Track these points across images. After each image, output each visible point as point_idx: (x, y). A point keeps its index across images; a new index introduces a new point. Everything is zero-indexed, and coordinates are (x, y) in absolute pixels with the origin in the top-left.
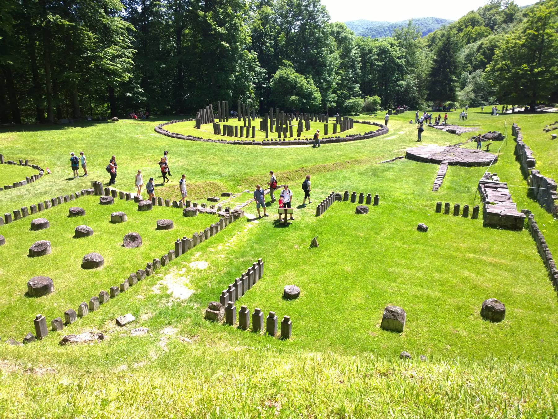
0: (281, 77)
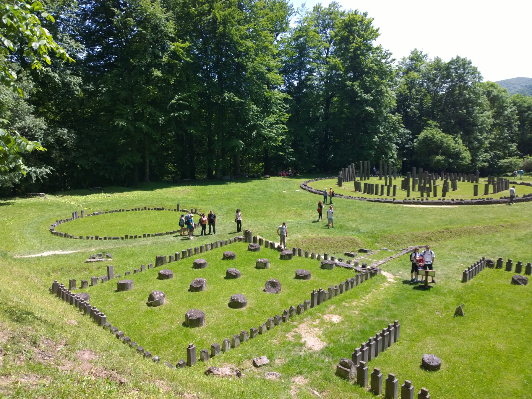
0: (426, 138)
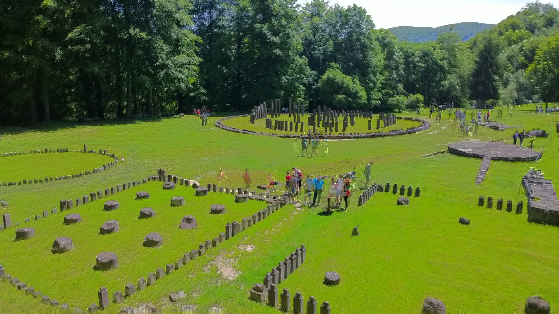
0: (329, 79)
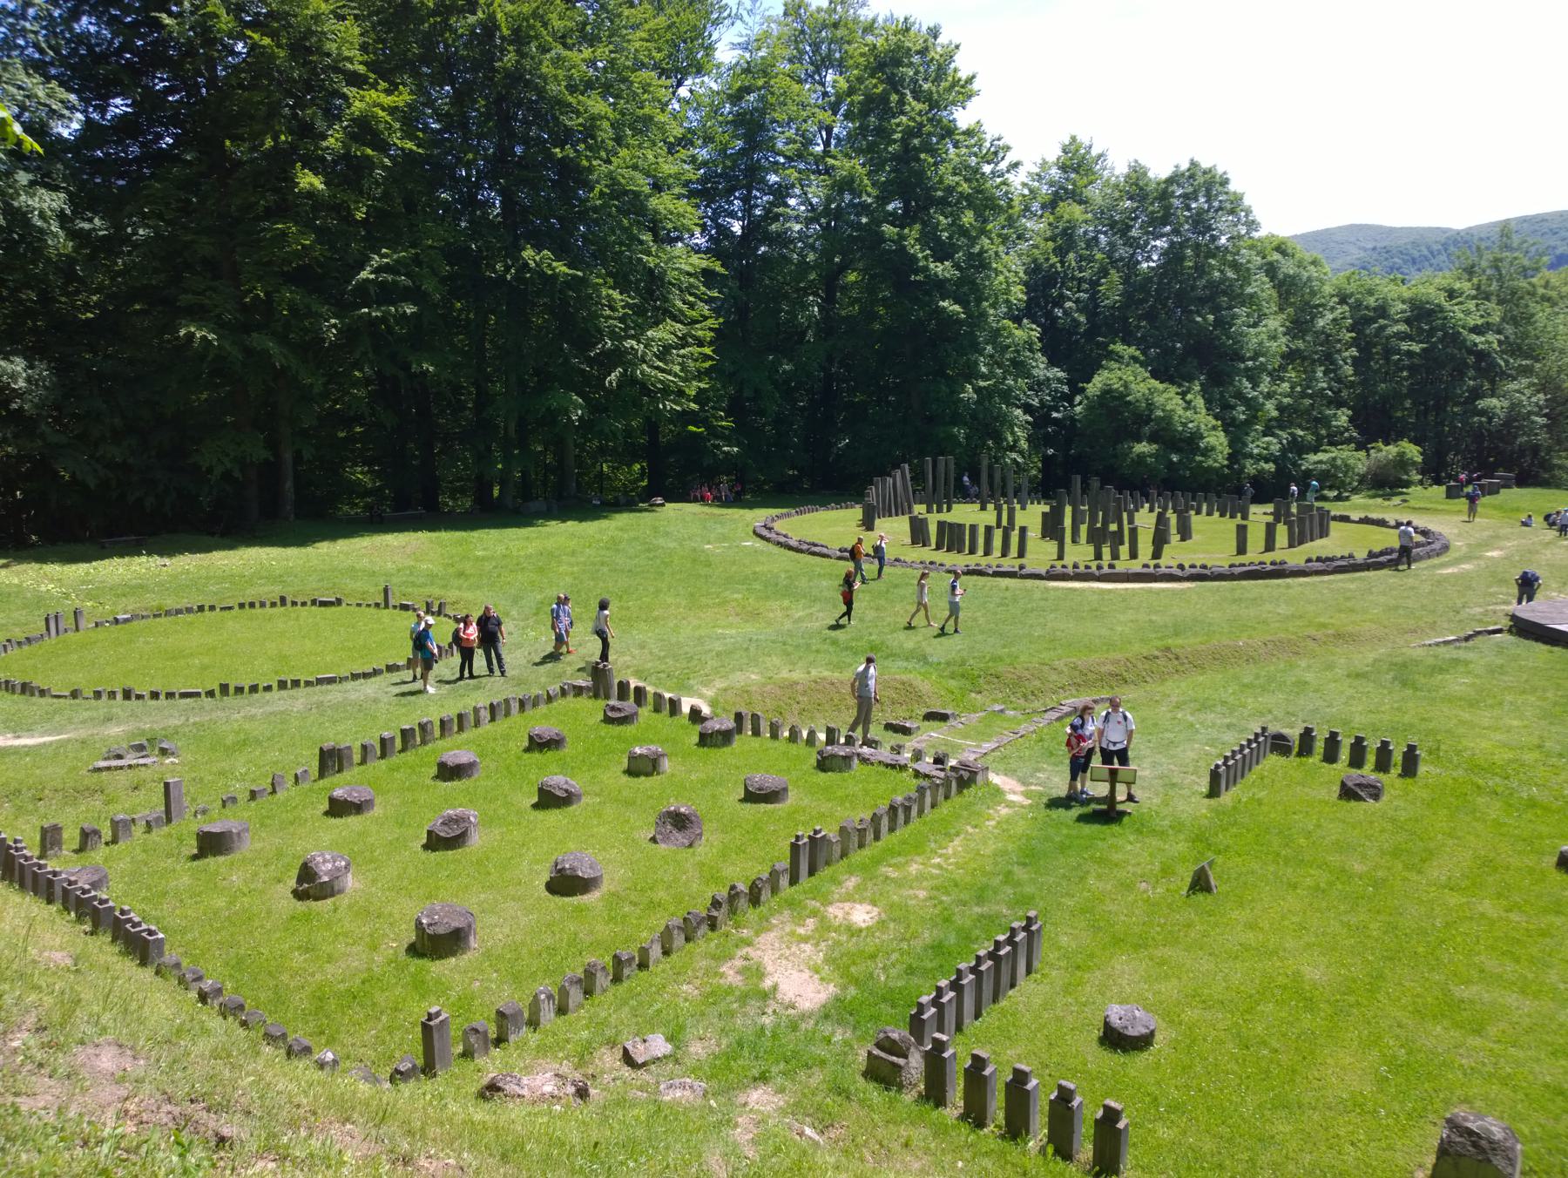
0: (1107, 392)
